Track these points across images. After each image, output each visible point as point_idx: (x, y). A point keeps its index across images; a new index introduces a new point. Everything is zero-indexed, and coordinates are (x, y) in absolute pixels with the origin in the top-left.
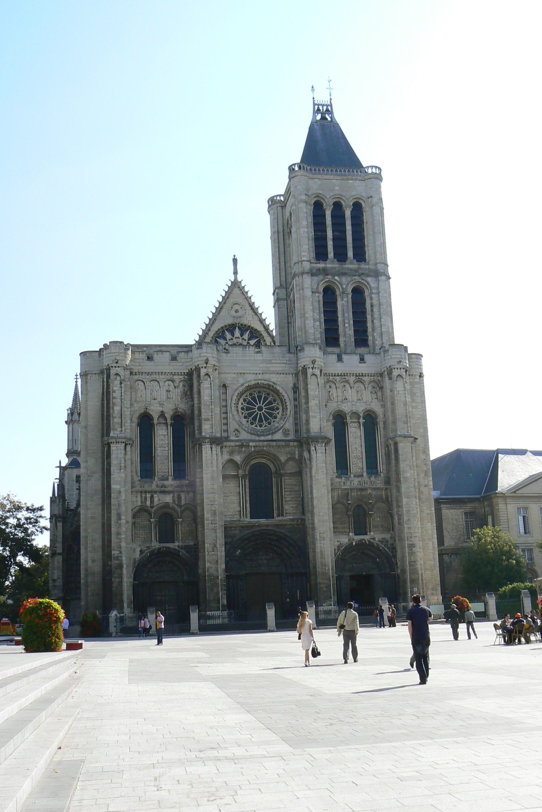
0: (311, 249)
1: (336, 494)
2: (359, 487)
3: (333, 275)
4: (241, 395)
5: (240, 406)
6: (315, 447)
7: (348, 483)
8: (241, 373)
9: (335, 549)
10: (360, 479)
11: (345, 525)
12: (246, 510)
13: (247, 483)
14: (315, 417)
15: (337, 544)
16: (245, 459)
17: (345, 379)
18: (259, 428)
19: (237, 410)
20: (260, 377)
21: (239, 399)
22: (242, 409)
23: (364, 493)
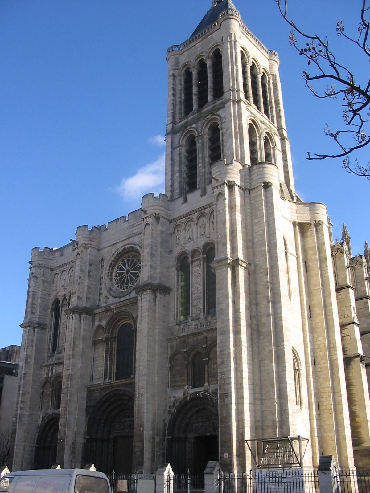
0: (178, 112)
1: (175, 343)
2: (196, 331)
3: (191, 125)
4: (113, 265)
5: (114, 274)
6: (141, 296)
7: (186, 329)
8: (114, 244)
9: (170, 407)
10: (197, 322)
11: (183, 378)
12: (110, 373)
13: (115, 345)
14: (146, 265)
15: (172, 399)
16: (109, 322)
17: (189, 218)
18: (126, 290)
19: (111, 279)
20: (126, 242)
21: (113, 269)
22: (116, 276)
23: (200, 337)
